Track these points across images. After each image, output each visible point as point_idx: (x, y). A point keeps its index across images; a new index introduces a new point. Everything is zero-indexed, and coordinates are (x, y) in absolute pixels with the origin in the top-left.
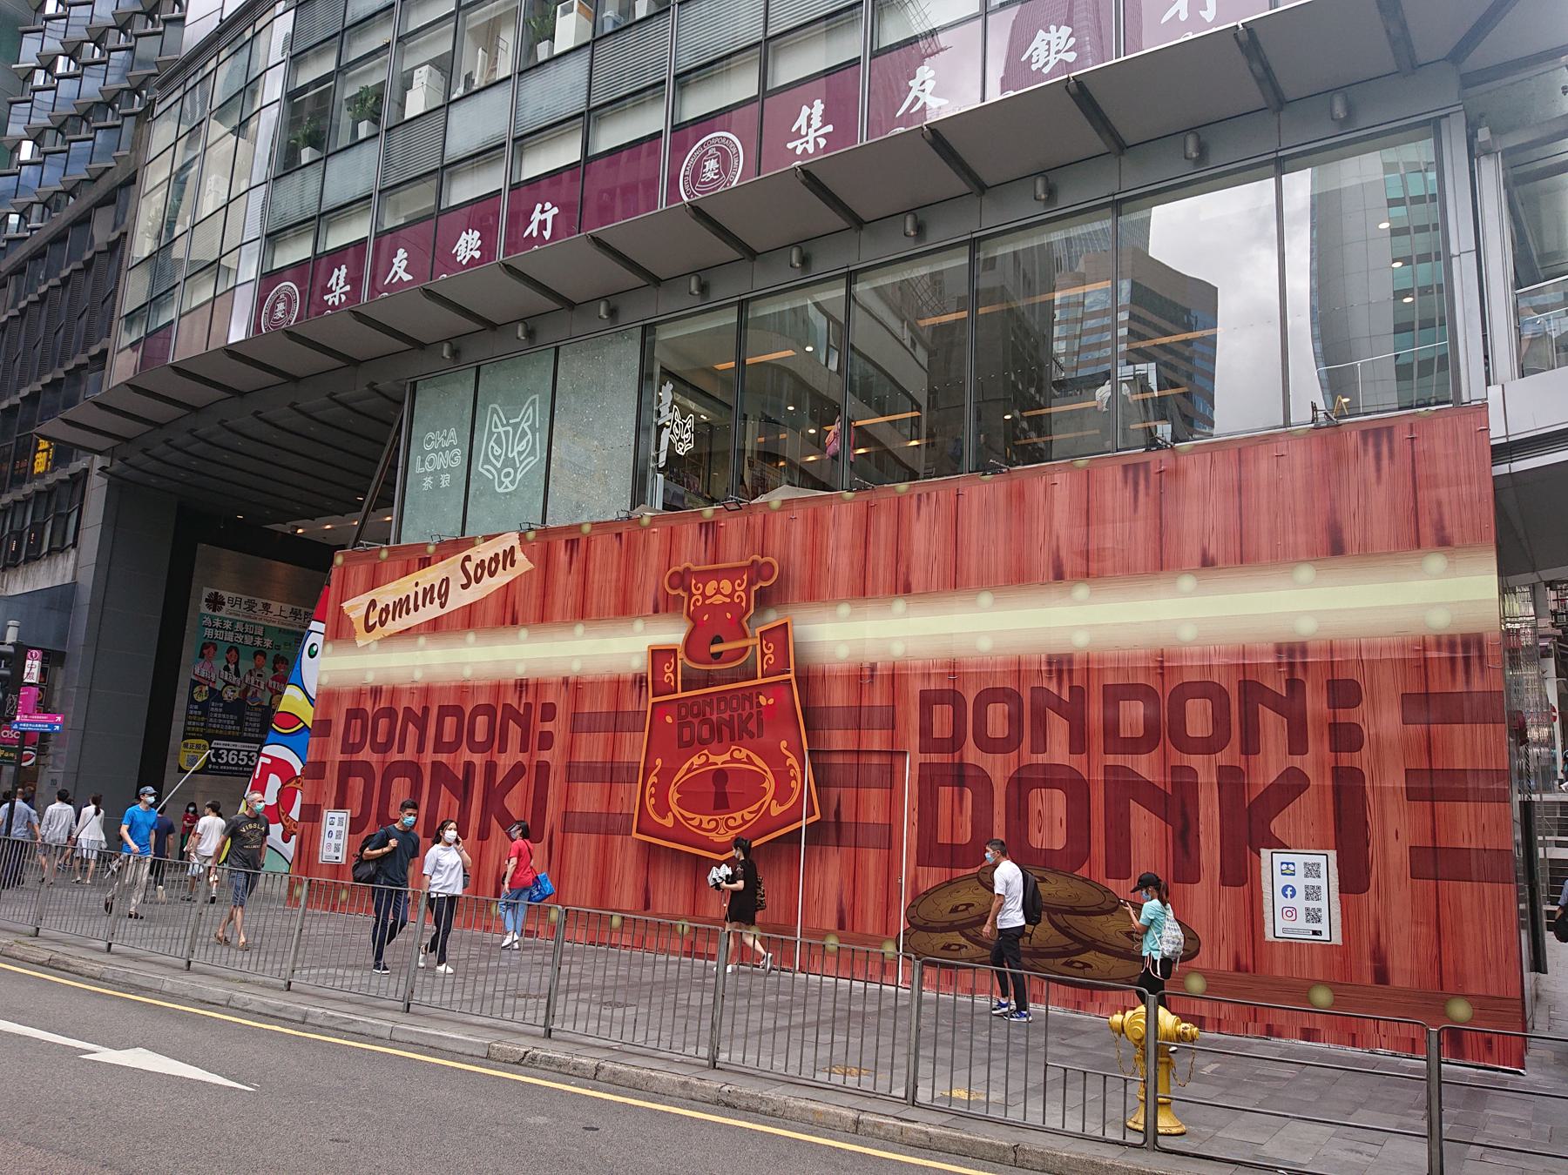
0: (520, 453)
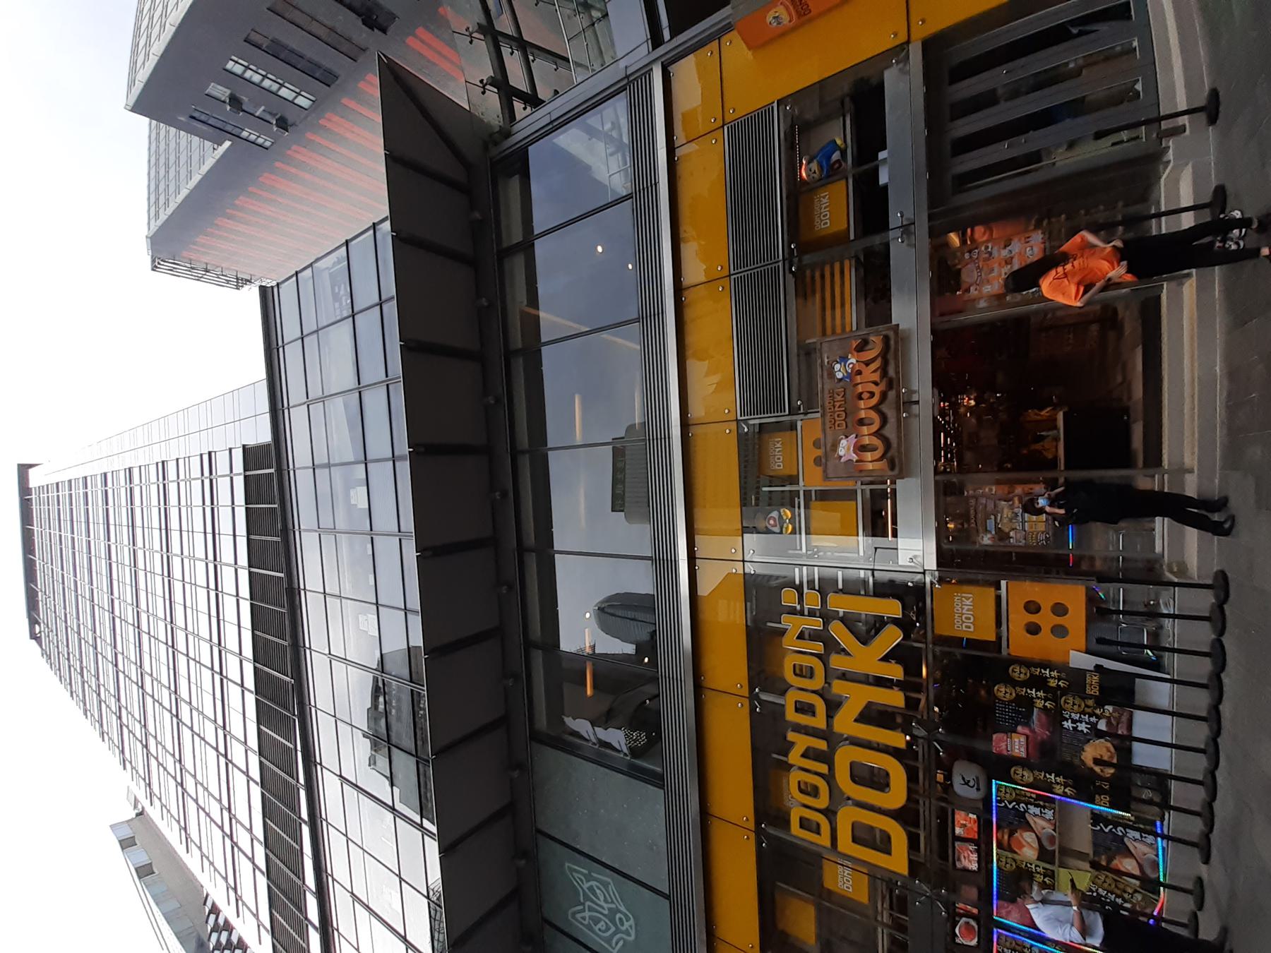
0: (606, 901)
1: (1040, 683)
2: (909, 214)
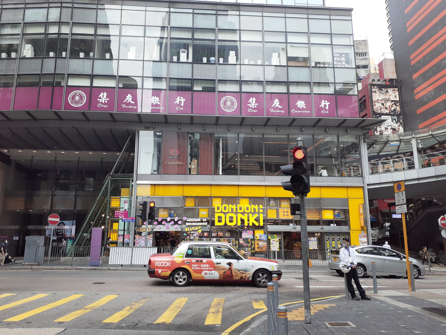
1: (252, 244)
2: (325, 229)
